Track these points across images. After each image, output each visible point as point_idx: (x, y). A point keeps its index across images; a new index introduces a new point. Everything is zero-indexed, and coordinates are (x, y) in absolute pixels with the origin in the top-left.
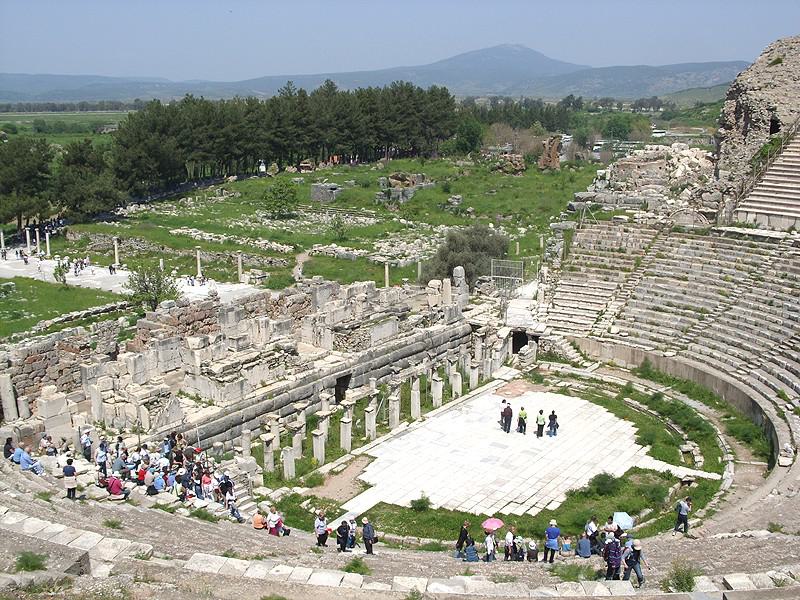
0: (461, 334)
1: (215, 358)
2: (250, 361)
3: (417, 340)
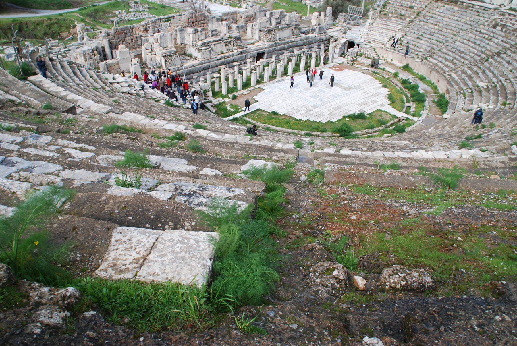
0: (324, 39)
1: (200, 39)
3: (301, 40)
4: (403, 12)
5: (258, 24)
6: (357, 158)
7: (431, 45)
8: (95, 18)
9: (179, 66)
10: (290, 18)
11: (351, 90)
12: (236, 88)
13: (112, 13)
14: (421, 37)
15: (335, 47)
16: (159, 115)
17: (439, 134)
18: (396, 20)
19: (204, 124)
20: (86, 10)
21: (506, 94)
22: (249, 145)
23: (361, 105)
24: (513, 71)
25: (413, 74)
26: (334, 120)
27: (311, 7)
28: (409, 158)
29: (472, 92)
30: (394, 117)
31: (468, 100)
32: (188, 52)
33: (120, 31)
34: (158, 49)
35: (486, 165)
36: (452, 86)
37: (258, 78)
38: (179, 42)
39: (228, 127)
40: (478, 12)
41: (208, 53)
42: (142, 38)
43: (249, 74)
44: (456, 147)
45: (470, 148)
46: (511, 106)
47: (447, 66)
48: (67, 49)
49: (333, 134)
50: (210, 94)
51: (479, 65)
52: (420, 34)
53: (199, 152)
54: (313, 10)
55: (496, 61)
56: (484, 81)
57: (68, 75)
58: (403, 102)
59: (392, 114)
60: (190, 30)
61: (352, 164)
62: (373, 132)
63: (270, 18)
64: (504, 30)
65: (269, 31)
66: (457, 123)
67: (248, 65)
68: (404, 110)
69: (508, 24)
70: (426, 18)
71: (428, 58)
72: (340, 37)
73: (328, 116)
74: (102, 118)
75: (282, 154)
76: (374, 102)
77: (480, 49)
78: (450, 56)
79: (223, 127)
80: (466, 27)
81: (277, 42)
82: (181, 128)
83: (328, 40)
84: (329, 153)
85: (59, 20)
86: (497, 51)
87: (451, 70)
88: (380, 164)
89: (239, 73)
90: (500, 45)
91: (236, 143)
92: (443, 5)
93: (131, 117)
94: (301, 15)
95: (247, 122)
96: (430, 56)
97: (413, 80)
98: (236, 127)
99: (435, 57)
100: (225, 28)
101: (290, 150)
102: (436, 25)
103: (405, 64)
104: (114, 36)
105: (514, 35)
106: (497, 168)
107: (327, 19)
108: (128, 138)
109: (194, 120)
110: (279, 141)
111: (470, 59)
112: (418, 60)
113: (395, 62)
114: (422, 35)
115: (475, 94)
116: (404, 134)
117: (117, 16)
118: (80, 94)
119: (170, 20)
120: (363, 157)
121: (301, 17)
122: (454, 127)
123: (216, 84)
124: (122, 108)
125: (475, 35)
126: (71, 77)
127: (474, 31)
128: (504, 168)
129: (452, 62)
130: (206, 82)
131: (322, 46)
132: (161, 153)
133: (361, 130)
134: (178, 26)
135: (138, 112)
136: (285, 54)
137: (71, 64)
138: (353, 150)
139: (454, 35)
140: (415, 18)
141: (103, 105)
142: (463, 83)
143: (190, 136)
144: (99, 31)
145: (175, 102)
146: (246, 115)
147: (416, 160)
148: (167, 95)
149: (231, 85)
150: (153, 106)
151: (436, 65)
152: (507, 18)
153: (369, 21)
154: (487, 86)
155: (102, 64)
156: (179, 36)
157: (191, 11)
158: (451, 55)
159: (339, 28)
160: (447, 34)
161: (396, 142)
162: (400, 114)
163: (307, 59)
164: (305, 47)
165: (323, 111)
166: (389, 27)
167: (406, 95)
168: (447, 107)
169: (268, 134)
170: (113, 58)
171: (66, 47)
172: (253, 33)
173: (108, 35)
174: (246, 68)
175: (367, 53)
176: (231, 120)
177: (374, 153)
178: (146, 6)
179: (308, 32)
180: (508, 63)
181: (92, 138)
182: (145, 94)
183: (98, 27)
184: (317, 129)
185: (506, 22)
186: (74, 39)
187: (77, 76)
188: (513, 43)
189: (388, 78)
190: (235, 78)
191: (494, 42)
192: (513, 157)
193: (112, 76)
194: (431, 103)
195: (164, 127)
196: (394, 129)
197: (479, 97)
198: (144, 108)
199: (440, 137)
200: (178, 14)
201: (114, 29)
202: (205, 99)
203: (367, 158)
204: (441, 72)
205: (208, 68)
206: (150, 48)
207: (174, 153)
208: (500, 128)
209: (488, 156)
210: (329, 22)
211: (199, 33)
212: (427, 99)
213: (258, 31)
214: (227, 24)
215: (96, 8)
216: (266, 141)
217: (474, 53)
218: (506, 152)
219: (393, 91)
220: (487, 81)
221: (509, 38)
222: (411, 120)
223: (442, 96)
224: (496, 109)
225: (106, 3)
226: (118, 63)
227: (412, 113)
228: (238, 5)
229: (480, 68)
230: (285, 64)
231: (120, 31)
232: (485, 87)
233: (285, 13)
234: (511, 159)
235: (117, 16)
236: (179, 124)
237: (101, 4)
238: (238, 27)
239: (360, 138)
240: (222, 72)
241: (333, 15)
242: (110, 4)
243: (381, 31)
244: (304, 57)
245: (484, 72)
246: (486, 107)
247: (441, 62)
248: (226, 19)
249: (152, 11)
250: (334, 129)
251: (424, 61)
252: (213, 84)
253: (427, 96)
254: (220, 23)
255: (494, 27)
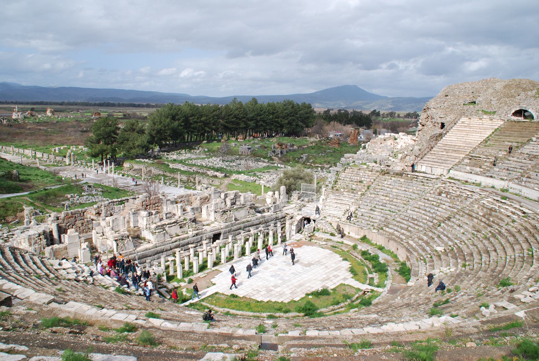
0: (280, 217)
1: (154, 222)
2: (170, 224)
3: (257, 219)
4: (354, 187)
5: (213, 205)
6: (324, 339)
7: (385, 216)
8: (45, 201)
9: (131, 250)
10: (245, 198)
11: (312, 266)
12: (192, 271)
13: (64, 196)
14: (374, 209)
15: (291, 224)
16: (108, 303)
17: (406, 304)
18: (348, 195)
19: (158, 312)
20: (37, 194)
21: (464, 256)
22: (206, 334)
23: (324, 281)
24: (465, 233)
25: (372, 244)
26: (297, 299)
27: (265, 186)
28: (379, 334)
29: (431, 257)
30: (359, 290)
31: (430, 266)
32: (143, 236)
33: (70, 215)
34: (109, 233)
35: (460, 332)
36: (411, 253)
37: (215, 260)
38: (132, 225)
39: (184, 313)
40: (422, 182)
41: (163, 236)
42: (94, 222)
43: (205, 256)
44: (426, 316)
45: (440, 314)
46: (471, 267)
47: (403, 234)
48: (10, 233)
49: (298, 314)
50: (165, 278)
51: (433, 230)
52: (373, 205)
53: (151, 344)
54: (267, 189)
55: (448, 225)
56: (441, 245)
57: (8, 262)
58: (365, 274)
59: (356, 287)
60: (144, 213)
61: (319, 346)
62: (339, 308)
63: (225, 199)
64: (449, 196)
65: (224, 212)
66: (423, 290)
67: (204, 246)
68: (368, 282)
69: (451, 191)
70: (376, 190)
71: (384, 228)
72: (296, 214)
73: (290, 295)
74: (42, 309)
75: (244, 342)
76: (336, 276)
77: (431, 215)
78: (404, 224)
79: (179, 314)
80: (414, 196)
81: (233, 222)
82: (131, 318)
83: (284, 217)
84: (294, 337)
85: (6, 203)
86: (446, 216)
87: (408, 237)
88: (350, 343)
89: (195, 255)
90: (448, 210)
91: (193, 332)
92: (390, 178)
93: (76, 308)
94: (255, 195)
95: (205, 307)
96: (385, 226)
97: (372, 251)
98: (193, 313)
99: (390, 226)
100: (180, 210)
101: (252, 336)
102: (387, 196)
103: (362, 236)
104: (64, 220)
105: (458, 200)
106: (471, 334)
107: (282, 197)
108: (70, 332)
109: (147, 308)
110: (240, 327)
111: (424, 225)
112: (374, 231)
113: (352, 234)
114: (375, 207)
115: (434, 258)
116: (371, 307)
117: (68, 199)
118: (18, 282)
119: (124, 203)
120: (331, 337)
121: (256, 197)
122: (420, 295)
123: (170, 268)
124: (66, 297)
125: (424, 202)
126: (10, 264)
127: (423, 200)
128: (478, 333)
129: (407, 230)
130: (160, 266)
131: (279, 224)
132: (107, 350)
133: (326, 307)
134: (131, 209)
135: (85, 301)
136: (242, 234)
137: (13, 250)
138: (320, 330)
139: (405, 204)
140: (366, 191)
141: (44, 295)
142: (421, 249)
143: (142, 327)
144: (48, 215)
145: (126, 289)
146: (203, 300)
147: (387, 335)
148: (117, 281)
149: (187, 268)
150: (102, 294)
151: (393, 234)
152: (449, 186)
153: (323, 197)
154: (445, 250)
155: (48, 250)
156: (132, 220)
157: (145, 194)
158: (406, 223)
159: (294, 205)
160: (398, 204)
161: (364, 316)
162: (365, 287)
163: (264, 237)
164: (262, 226)
165: (285, 290)
166: (342, 202)
167: (367, 267)
168: (409, 274)
169: (227, 319)
170: (60, 242)
171: (10, 231)
172: (208, 215)
173: (58, 219)
174: (202, 250)
175: (324, 228)
176: (187, 306)
177: (342, 331)
178: (100, 189)
179: (264, 211)
180: (459, 226)
181: (26, 336)
182: (93, 281)
183: (47, 210)
184: (280, 310)
185: (449, 189)
186: (20, 222)
187: (19, 263)
188: (459, 208)
189: (348, 251)
190: (191, 261)
191: (442, 208)
192: (484, 319)
193: (58, 261)
194: (394, 272)
195: (113, 318)
196: (360, 303)
197: (439, 261)
198: (91, 297)
199: (408, 307)
200: (132, 197)
201: (64, 213)
202: (159, 284)
203: (335, 338)
204: (399, 241)
205: (162, 252)
206: (101, 232)
207: (122, 349)
208: (465, 291)
209: (459, 321)
210: (284, 201)
211: (153, 216)
212: (389, 268)
213: (213, 213)
214: (182, 207)
215: (47, 191)
216: (225, 328)
217: (426, 219)
218: (477, 315)
219: (354, 264)
220: (443, 245)
221: (455, 203)
222: (376, 291)
223: (404, 264)
224: (458, 272)
225: (58, 186)
226: (66, 248)
227: (376, 284)
228: (193, 187)
229: (435, 233)
230: (243, 244)
231: (70, 215)
232: (443, 251)
233: (240, 194)
234: (483, 322)
235: (68, 199)
236: (130, 313)
237: (53, 188)
238: (193, 209)
239: (326, 316)
240: (177, 255)
241: (287, 193)
242: (63, 188)
243: (336, 205)
244: (262, 236)
245: (439, 237)
246: (448, 271)
247: (397, 231)
248: (181, 202)
249: (105, 194)
250: (298, 309)
251: (381, 231)
252: (167, 267)
253: (388, 266)
254: (175, 205)
255: (440, 194)
